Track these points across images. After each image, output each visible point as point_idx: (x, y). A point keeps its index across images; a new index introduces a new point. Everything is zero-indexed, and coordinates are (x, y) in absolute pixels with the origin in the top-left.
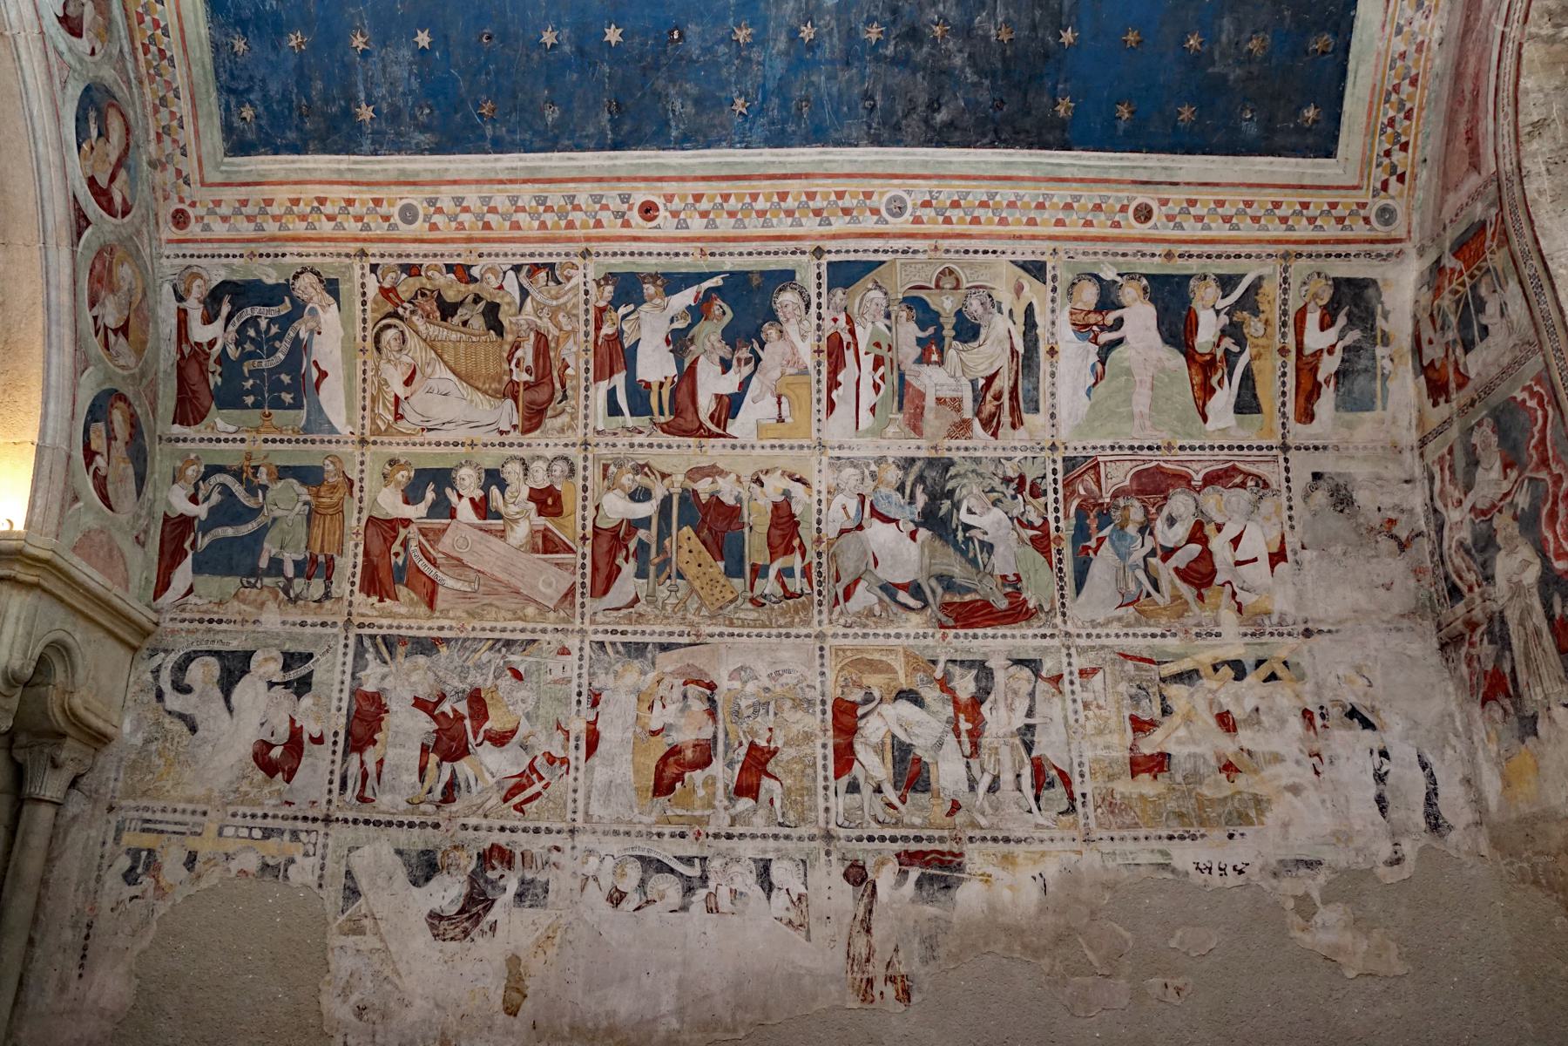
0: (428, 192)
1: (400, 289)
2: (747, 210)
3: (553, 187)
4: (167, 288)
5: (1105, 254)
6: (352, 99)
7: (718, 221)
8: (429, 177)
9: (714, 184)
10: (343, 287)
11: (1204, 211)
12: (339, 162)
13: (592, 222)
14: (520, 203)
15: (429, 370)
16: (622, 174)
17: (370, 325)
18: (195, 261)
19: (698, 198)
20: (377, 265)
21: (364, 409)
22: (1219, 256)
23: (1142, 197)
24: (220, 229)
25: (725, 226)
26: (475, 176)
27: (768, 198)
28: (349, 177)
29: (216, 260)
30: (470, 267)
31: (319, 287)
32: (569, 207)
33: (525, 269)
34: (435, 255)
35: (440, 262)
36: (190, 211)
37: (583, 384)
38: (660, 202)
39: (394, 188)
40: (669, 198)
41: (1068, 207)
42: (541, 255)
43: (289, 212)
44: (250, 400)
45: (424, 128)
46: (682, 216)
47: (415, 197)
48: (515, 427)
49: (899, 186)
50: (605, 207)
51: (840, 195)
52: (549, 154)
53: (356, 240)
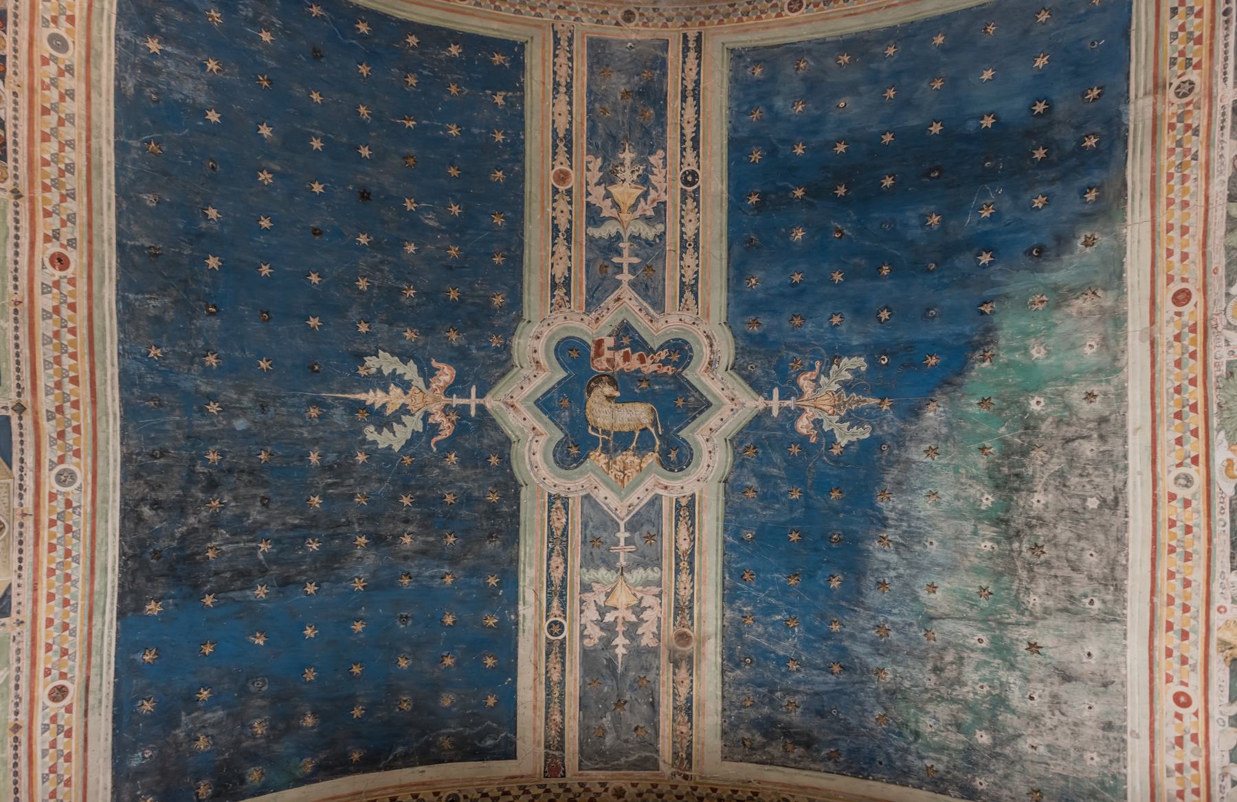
2: (62, 348)
5: (18, 669)
7: (50, 321)
9: (85, 324)
11: (60, 746)
13: (49, 208)
16: (96, 246)
19: (72, 307)
22: (16, 774)
23: (74, 689)
25: (45, 328)
27: (72, 368)
38: (69, 273)
40: (72, 282)
41: (65, 627)
46: (55, 291)
49: (85, 479)
50: (63, 224)
51: (77, 430)
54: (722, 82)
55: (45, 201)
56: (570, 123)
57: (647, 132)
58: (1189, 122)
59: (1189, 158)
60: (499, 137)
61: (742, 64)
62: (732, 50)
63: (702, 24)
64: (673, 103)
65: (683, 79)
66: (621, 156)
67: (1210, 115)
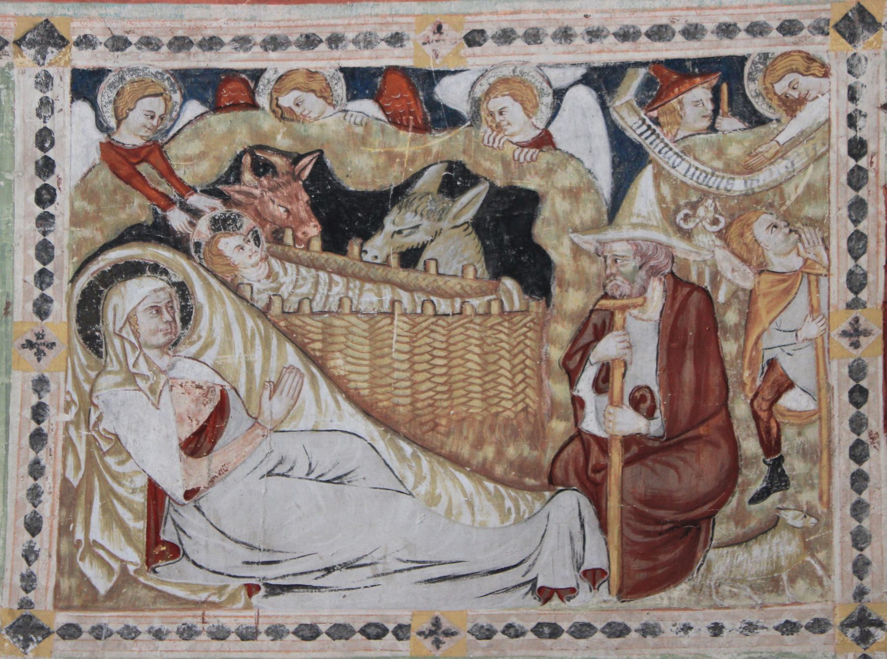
1: (176, 151)
15: (275, 407)
20: (100, 74)
21: (34, 526)
34: (309, 42)
37: (844, 437)
48: (594, 577)
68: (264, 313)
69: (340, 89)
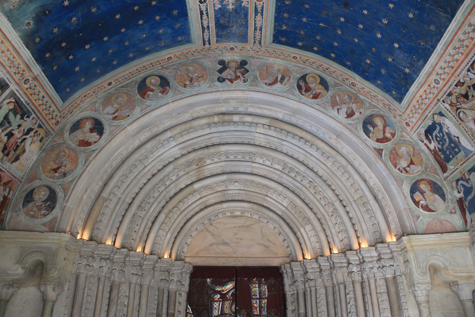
0: (434, 73)
1: (453, 101)
3: (453, 42)
4: (419, 141)
6: (403, 71)
8: (431, 70)
10: (443, 112)
12: (415, 85)
13: (470, 40)
14: (452, 54)
17: (455, 116)
18: (417, 131)
20: (443, 100)
24: (414, 120)
26: (438, 59)
28: (420, 86)
29: (420, 127)
30: (459, 81)
31: (439, 116)
32: (462, 43)
33: (470, 68)
34: (451, 86)
35: (453, 86)
36: (407, 121)
39: (429, 79)
42: (470, 61)
43: (419, 105)
44: (451, 156)
45: (418, 60)
47: (433, 77)
50: (469, 33)
52: (444, 36)
53: (434, 98)
54: (193, 34)
55: (470, 43)
56: (255, 18)
57: (223, 15)
58: (19, 75)
59: (12, 65)
60: (286, 15)
61: (187, 39)
62: (191, 43)
63: (204, 48)
64: (212, 25)
65: (209, 32)
66: (233, 7)
67: (14, 80)
68: (469, 109)
69: (456, 87)
